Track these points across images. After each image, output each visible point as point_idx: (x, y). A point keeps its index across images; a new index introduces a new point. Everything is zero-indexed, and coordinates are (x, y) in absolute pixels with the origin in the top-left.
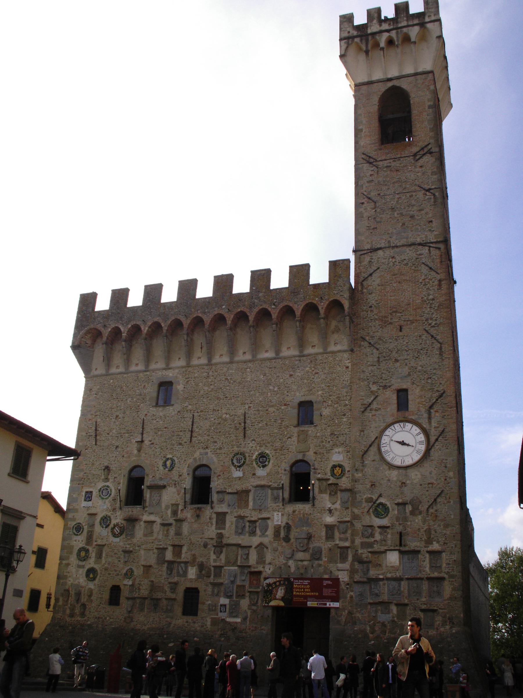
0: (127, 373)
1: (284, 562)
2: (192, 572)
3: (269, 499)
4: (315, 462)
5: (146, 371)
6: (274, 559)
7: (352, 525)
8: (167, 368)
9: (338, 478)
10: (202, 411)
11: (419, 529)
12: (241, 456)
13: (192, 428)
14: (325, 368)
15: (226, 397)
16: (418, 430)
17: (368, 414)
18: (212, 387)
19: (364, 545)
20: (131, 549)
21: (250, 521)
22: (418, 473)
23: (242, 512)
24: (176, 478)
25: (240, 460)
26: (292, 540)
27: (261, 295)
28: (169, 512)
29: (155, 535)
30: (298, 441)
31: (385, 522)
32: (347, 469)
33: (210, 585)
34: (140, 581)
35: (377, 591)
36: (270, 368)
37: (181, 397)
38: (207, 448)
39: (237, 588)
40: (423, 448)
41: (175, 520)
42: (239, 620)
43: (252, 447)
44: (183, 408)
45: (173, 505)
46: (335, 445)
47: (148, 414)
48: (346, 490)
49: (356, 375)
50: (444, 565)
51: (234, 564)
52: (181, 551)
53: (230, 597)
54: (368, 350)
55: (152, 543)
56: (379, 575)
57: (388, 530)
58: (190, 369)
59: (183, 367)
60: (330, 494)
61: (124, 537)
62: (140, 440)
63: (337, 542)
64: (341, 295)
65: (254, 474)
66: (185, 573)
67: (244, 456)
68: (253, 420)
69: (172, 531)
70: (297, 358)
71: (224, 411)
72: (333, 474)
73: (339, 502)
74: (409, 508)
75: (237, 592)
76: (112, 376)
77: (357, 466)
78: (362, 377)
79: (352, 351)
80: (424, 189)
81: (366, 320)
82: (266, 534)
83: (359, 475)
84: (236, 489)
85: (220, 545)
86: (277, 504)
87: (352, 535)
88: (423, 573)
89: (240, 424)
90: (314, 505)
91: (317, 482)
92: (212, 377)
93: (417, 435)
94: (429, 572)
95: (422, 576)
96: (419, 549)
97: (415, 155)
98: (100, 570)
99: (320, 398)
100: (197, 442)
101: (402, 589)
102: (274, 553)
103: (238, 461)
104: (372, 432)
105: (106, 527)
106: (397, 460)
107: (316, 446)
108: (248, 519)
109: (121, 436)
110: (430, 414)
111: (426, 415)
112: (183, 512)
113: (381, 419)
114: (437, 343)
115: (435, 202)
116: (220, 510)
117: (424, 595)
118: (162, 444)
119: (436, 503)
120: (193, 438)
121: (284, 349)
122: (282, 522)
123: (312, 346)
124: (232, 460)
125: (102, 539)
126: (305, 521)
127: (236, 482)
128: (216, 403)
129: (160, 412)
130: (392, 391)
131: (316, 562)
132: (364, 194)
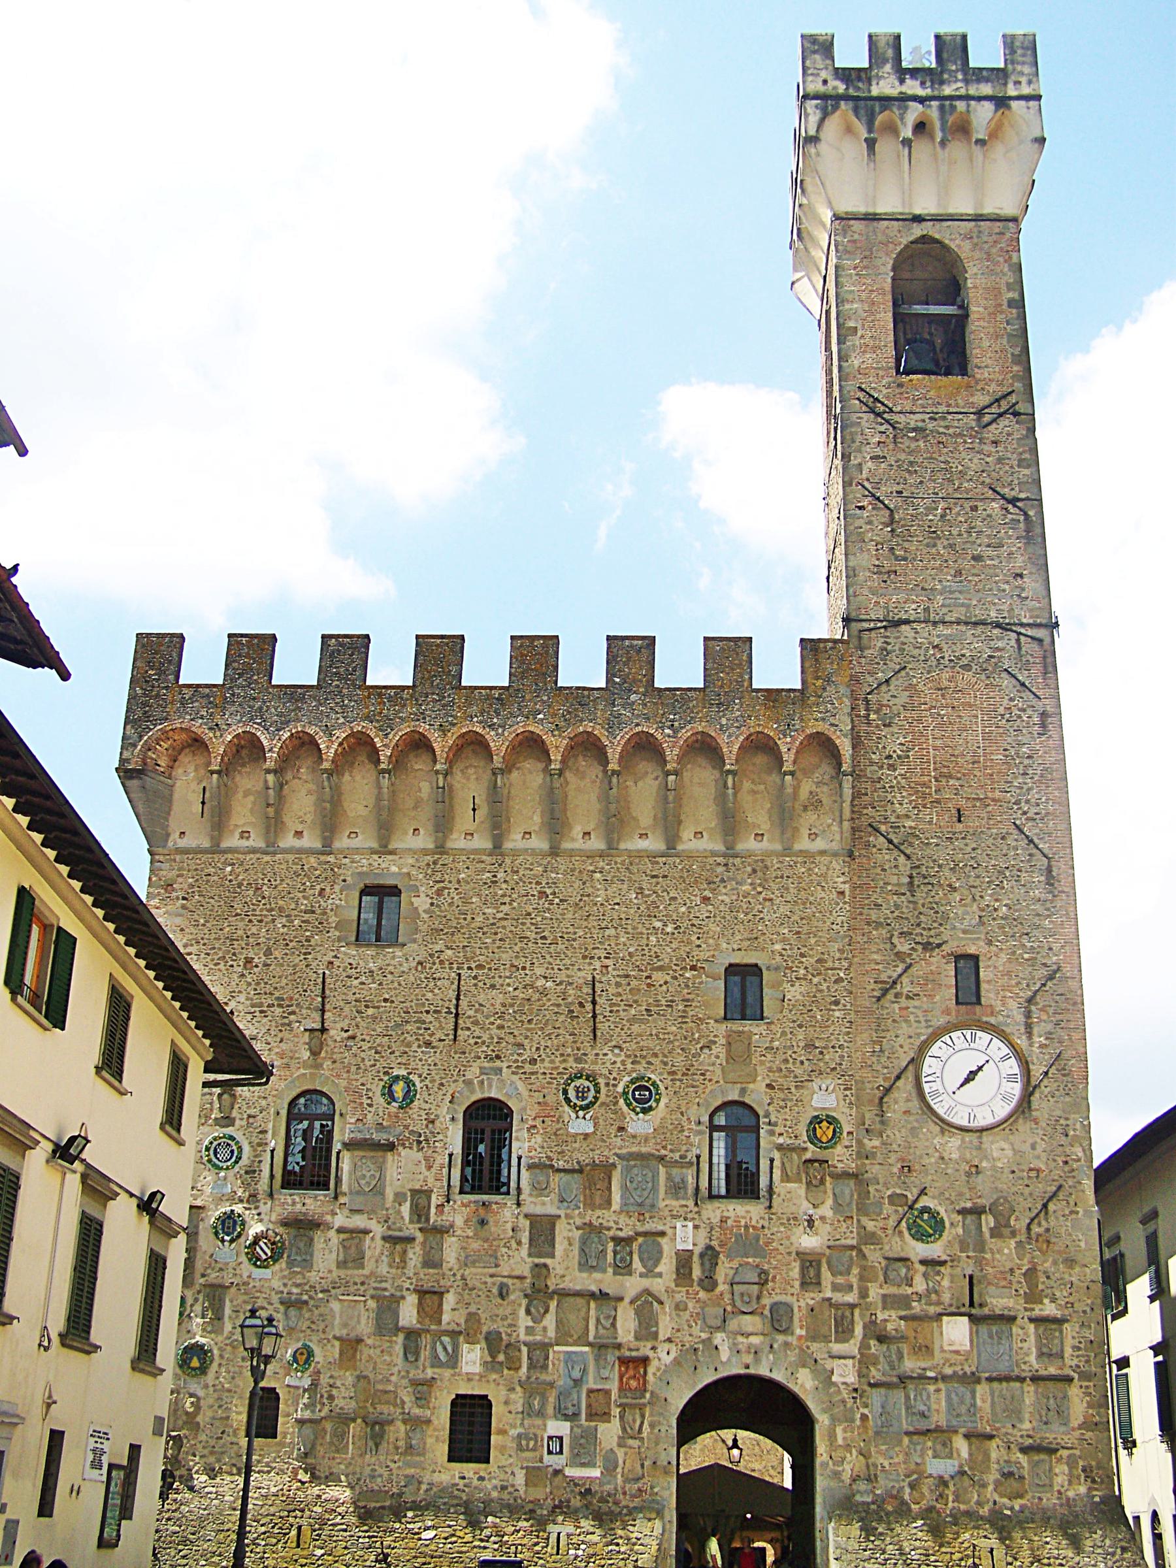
0: (274, 853)
1: (704, 1336)
2: (472, 1357)
3: (662, 1190)
4: (771, 1108)
5: (323, 853)
6: (678, 1330)
8: (384, 849)
9: (826, 1148)
10: (480, 967)
11: (1012, 1270)
12: (587, 1083)
13: (457, 1006)
14: (787, 889)
15: (544, 938)
16: (1006, 1050)
18: (505, 908)
19: (888, 1301)
20: (305, 1297)
21: (617, 1240)
22: (1006, 1146)
23: (593, 1216)
25: (582, 1091)
26: (722, 1287)
27: (633, 697)
28: (406, 1209)
30: (730, 1057)
31: (935, 1250)
33: (518, 1389)
34: (331, 1377)
35: (923, 1408)
37: (424, 928)
38: (498, 1057)
39: (588, 1396)
40: (1016, 1089)
41: (420, 1229)
42: (596, 1473)
43: (615, 1062)
44: (431, 956)
45: (414, 1192)
47: (337, 963)
48: (846, 1175)
49: (861, 914)
50: (1068, 1351)
51: (583, 1340)
52: (441, 1305)
53: (573, 1417)
54: (887, 857)
55: (363, 1283)
56: (924, 1369)
57: (942, 1269)
59: (425, 852)
60: (809, 1184)
61: (284, 1265)
62: (317, 1026)
63: (828, 1294)
64: (832, 725)
65: (621, 1129)
66: (453, 1360)
67: (596, 1085)
69: (415, 1255)
70: (719, 860)
71: (539, 971)
72: (813, 1138)
74: (988, 1221)
75: (589, 1406)
76: (230, 856)
77: (867, 1122)
78: (874, 918)
79: (851, 855)
80: (1003, 497)
81: (878, 786)
82: (657, 1270)
83: (872, 1143)
84: (578, 1163)
85: (540, 1293)
86: (684, 1202)
87: (862, 1278)
88: (1023, 1367)
89: (581, 1005)
90: (770, 1207)
91: (777, 1155)
92: (504, 886)
93: (1004, 1059)
94: (1036, 1366)
95: (1024, 1375)
96: (1012, 1313)
97: (980, 413)
98: (220, 1349)
99: (778, 958)
100: (472, 1041)
101: (979, 1402)
102: (678, 1315)
103: (581, 1093)
104: (901, 1046)
105: (232, 1241)
106: (959, 1115)
107: (770, 1070)
108: (611, 1233)
109: (261, 1012)
110: (1028, 1015)
111: (1020, 1018)
112: (442, 1212)
113: (922, 1019)
115: (1028, 531)
116: (539, 1210)
117: (1027, 1416)
118: (378, 1041)
119: (1046, 1213)
120: (459, 1032)
121: (687, 834)
122: (694, 1245)
123: (756, 835)
124: (565, 1092)
125: (221, 1269)
126: (749, 1242)
127: (577, 1145)
128: (517, 949)
129: (369, 959)
130: (944, 957)
131: (781, 1338)
132: (863, 486)
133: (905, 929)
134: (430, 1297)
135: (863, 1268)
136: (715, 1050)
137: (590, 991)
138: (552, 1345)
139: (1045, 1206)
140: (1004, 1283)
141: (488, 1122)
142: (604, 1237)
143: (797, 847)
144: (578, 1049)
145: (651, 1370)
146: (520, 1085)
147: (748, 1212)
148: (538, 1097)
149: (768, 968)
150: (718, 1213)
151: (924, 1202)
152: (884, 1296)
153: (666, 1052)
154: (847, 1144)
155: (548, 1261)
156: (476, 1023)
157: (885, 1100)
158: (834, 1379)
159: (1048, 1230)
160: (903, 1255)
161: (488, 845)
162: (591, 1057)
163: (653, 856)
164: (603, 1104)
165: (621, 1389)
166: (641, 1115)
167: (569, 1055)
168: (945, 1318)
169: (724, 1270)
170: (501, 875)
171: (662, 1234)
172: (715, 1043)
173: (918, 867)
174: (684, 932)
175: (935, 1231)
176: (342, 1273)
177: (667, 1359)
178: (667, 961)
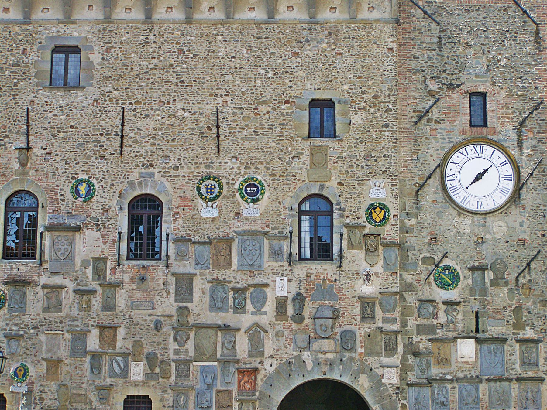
1: (295, 353)
2: (137, 370)
3: (266, 255)
4: (341, 199)
5: (25, 23)
6: (278, 350)
7: (403, 298)
8: (68, 20)
9: (378, 226)
10: (138, 102)
12: (213, 183)
13: (122, 130)
14: (353, 46)
15: (182, 82)
16: (503, 159)
17: (425, 129)
18: (155, 61)
19: (420, 329)
20: (21, 333)
21: (236, 290)
22: (502, 224)
23: (219, 274)
24: (98, 214)
25: (210, 188)
26: (307, 321)
28: (89, 271)
29: (65, 310)
30: (313, 164)
32: (393, 212)
33: (169, 391)
34: (41, 385)
35: (443, 399)
36: (259, 38)
38: (151, 165)
40: (510, 185)
41: (100, 285)
43: (233, 168)
45: (95, 260)
46: (372, 174)
47: (36, 101)
48: (392, 244)
49: (404, 64)
50: (541, 361)
51: (212, 357)
52: (115, 336)
54: (423, 24)
55: (61, 322)
56: (445, 374)
57: (458, 307)
58: (112, 27)
59: (97, 22)
60: (367, 250)
61: (6, 311)
62: (24, 145)
63: (380, 325)
65: (238, 214)
67: (220, 184)
68: (233, 124)
69: (96, 302)
70: (305, 26)
71: (179, 105)
72: (370, 219)
73: (381, 263)
74: (489, 275)
75: (218, 401)
79: (397, 22)
83: (411, 223)
84: (208, 237)
85: (183, 326)
86: (281, 264)
87: (402, 314)
88: (511, 372)
90: (340, 266)
91: (345, 231)
92: (154, 45)
93: (503, 164)
94: (520, 372)
95: (511, 377)
96: (504, 337)
99: (346, 95)
100: (133, 155)
101: (481, 396)
102: (278, 340)
103: (210, 190)
104: (431, 156)
106: (471, 202)
107: (341, 172)
108: (231, 285)
110: (520, 134)
111: (514, 136)
112: (115, 273)
113: (446, 137)
114: (531, 23)
116: (181, 270)
117: (513, 403)
118: (67, 156)
119: (529, 270)
120: (124, 148)
121: (282, 8)
123: (331, 8)
124: (199, 189)
126: (326, 290)
127: (207, 226)
130: (462, 94)
131: (347, 354)
133: (435, 75)
134: (108, 331)
135: (404, 307)
136: (303, 159)
137: (216, 119)
138: (191, 361)
139: (528, 265)
140: (499, 317)
141: (145, 210)
142: (226, 288)
143: (360, 16)
144: (207, 159)
145: (259, 377)
146: (168, 186)
148: (180, 192)
149: (339, 102)
150: (305, 271)
152: (418, 326)
153: (268, 161)
154: (393, 223)
155: (189, 305)
156: (136, 142)
157: (420, 193)
158: (383, 381)
159: (530, 281)
160: (431, 298)
161: (141, 16)
162: (216, 165)
163: (258, 24)
164: (225, 197)
165: (240, 390)
166: (251, 204)
167: (201, 163)
168: (459, 340)
169: (309, 309)
170: (151, 38)
171: (267, 285)
172: (302, 154)
173: (444, 31)
174: (281, 77)
175: (453, 282)
176: (47, 315)
177: (271, 370)
178: (268, 97)
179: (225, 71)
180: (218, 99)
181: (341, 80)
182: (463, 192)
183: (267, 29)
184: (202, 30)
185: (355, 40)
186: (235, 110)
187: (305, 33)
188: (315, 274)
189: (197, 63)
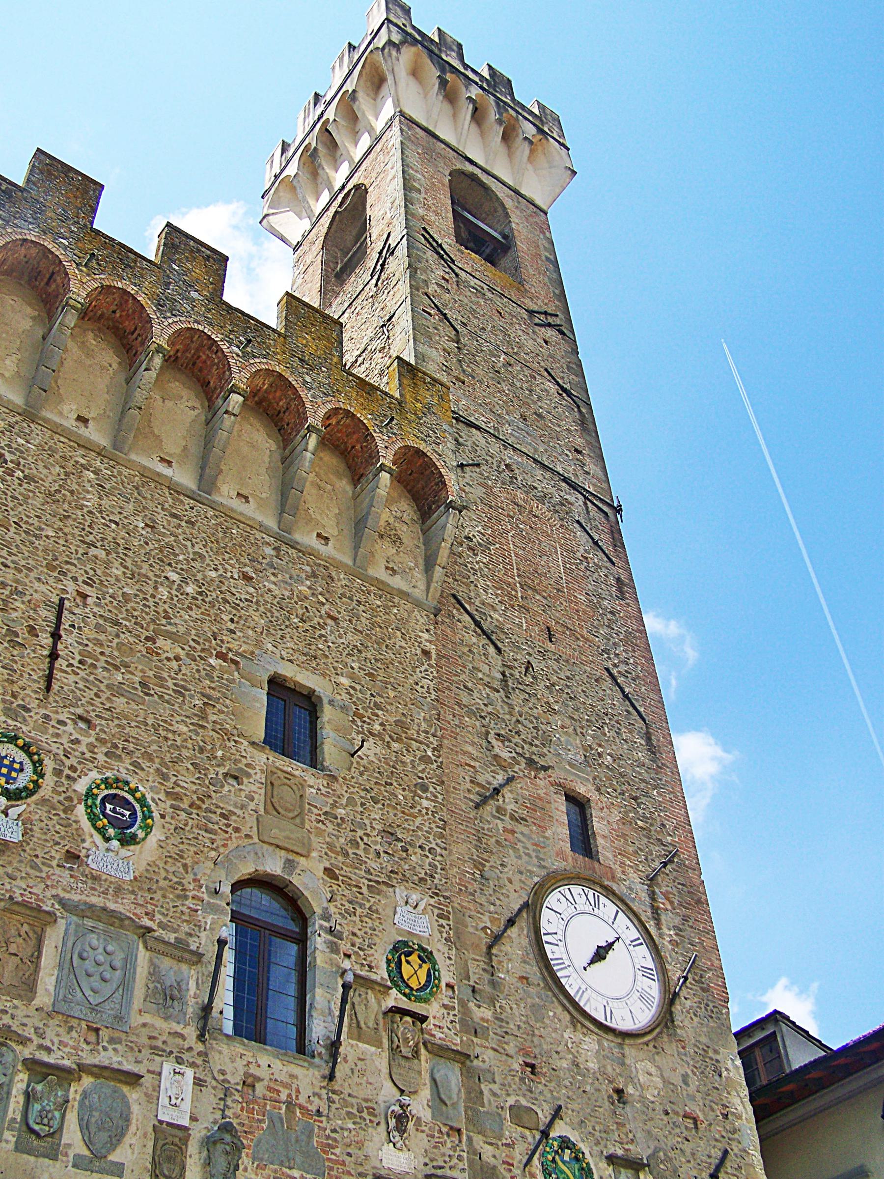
12: (20, 756)
21: (39, 1070)
60: (394, 1050)
70: (268, 539)
89: (32, 630)
90: (331, 1077)
107: (331, 846)
108: (27, 1052)
111: (644, 896)
122: (193, 1119)
133: (503, 732)
136: (248, 786)
137: (53, 618)
144: (14, 696)
147: (292, 1076)
149: (331, 702)
150: (240, 1063)
151: (560, 1130)
153: (167, 759)
157: (494, 951)
164: (44, 801)
166: (115, 843)
171: (133, 1079)
172: (249, 775)
178: (182, 630)
179: (91, 537)
180: (65, 582)
181: (336, 664)
182: (575, 975)
183: (192, 508)
184: (55, 444)
185: (362, 608)
186: (101, 622)
187: (269, 551)
188: (266, 1083)
189: (31, 494)
